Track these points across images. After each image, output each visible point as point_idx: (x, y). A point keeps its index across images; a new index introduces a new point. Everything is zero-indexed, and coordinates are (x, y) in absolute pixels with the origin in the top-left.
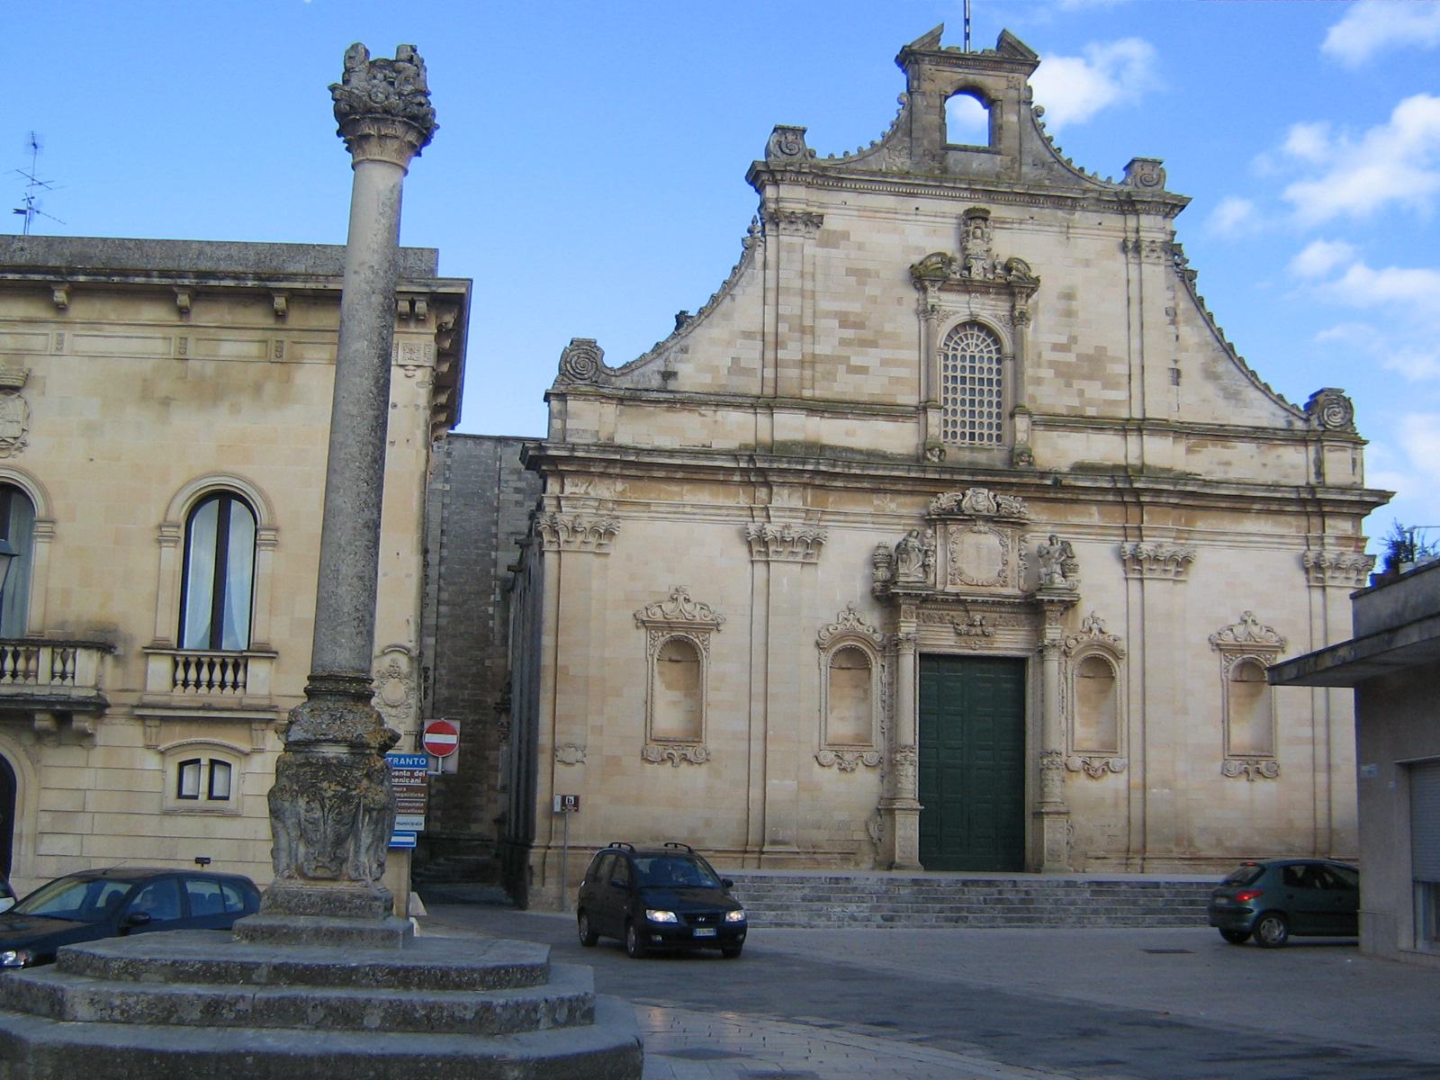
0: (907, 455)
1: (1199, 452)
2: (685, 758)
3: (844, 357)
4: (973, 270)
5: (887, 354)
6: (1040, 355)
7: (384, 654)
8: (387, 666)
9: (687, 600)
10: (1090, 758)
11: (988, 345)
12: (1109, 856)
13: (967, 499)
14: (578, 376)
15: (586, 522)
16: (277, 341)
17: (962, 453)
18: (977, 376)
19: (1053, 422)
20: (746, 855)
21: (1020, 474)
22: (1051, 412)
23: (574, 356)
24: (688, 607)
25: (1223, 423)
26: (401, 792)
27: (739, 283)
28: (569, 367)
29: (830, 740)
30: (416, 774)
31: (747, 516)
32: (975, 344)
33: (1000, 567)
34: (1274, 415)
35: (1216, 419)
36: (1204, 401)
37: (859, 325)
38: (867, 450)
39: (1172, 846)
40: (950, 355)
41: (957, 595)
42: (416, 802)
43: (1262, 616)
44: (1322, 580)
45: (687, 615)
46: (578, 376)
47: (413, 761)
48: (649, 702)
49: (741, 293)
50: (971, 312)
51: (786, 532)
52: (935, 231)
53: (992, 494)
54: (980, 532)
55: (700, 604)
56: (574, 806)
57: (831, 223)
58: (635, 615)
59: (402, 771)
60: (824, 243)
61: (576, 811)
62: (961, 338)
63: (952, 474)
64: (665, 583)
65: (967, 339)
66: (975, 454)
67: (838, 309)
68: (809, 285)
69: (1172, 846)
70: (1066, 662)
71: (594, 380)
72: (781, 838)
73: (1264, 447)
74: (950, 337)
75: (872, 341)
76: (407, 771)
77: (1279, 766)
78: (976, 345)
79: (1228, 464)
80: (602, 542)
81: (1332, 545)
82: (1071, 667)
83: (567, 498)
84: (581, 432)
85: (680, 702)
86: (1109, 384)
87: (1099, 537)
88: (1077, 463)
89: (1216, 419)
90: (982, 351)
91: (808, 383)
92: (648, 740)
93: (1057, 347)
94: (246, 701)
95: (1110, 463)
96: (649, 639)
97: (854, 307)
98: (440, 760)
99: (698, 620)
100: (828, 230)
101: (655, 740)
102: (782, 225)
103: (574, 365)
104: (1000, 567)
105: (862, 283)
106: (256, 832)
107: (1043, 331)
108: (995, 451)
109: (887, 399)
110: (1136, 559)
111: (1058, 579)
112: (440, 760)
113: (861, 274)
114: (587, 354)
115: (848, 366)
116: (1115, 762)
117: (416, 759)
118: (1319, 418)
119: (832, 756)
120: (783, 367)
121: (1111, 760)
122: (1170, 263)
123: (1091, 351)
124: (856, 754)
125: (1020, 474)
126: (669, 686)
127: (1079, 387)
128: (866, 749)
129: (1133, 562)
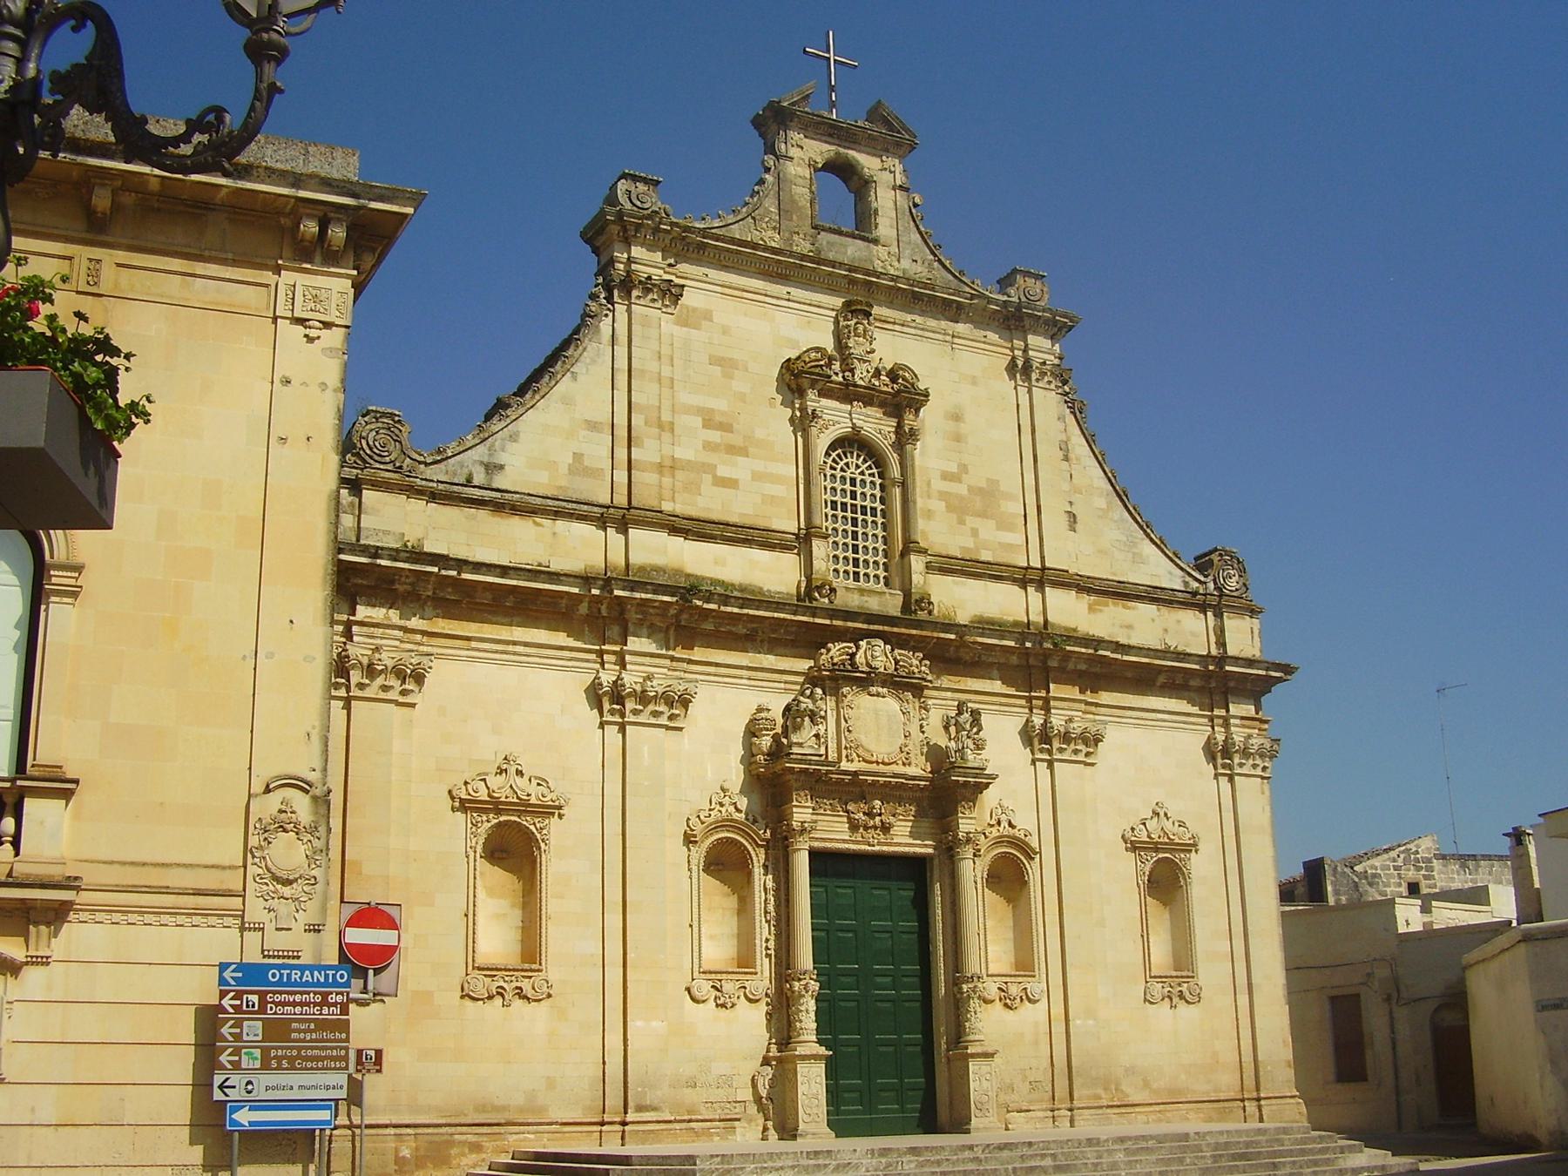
0: (788, 594)
1: (1101, 611)
2: (520, 993)
3: (709, 465)
4: (857, 372)
5: (759, 465)
6: (929, 484)
7: (268, 790)
8: (275, 812)
9: (520, 773)
10: (1006, 983)
11: (870, 467)
12: (1032, 1108)
13: (861, 652)
14: (376, 458)
15: (387, 659)
16: (90, 260)
17: (850, 595)
18: (858, 502)
19: (948, 566)
20: (604, 1128)
21: (919, 624)
22: (944, 553)
23: (372, 430)
24: (521, 783)
25: (1121, 579)
26: (304, 1031)
27: (582, 358)
28: (365, 446)
29: (705, 967)
30: (332, 998)
31: (595, 662)
32: (855, 464)
33: (902, 740)
34: (1170, 573)
35: (1115, 575)
36: (1100, 551)
37: (725, 427)
38: (740, 585)
39: (1100, 1091)
40: (828, 474)
41: (855, 774)
42: (332, 1048)
43: (1175, 808)
44: (1230, 767)
45: (519, 792)
46: (376, 458)
47: (327, 976)
48: (470, 916)
49: (584, 371)
50: (853, 424)
51: (649, 683)
52: (809, 322)
53: (888, 647)
54: (878, 695)
55: (536, 778)
56: (375, 1064)
57: (690, 298)
58: (450, 792)
59: (308, 993)
60: (684, 322)
61: (379, 1071)
62: (838, 455)
63: (831, 619)
64: (489, 751)
65: (846, 458)
66: (866, 598)
67: (701, 405)
68: (666, 371)
69: (1100, 1091)
70: (974, 863)
71: (398, 465)
72: (648, 1103)
73: (1164, 609)
74: (827, 454)
75: (741, 448)
76: (315, 993)
77: (1201, 989)
78: (857, 465)
79: (1130, 627)
80: (406, 686)
81: (1237, 726)
82: (980, 868)
83: (361, 624)
84: (381, 534)
85: (504, 915)
86: (1003, 525)
87: (1002, 708)
88: (975, 616)
89: (1115, 575)
90: (862, 473)
91: (667, 493)
92: (470, 968)
93: (946, 476)
94: (21, 869)
95: (1011, 619)
96: (469, 825)
97: (720, 404)
98: (371, 972)
99: (533, 800)
100: (687, 307)
101: (479, 969)
102: (635, 293)
103: (371, 443)
104: (902, 740)
105: (729, 377)
106: (33, 1110)
107: (929, 457)
108: (887, 595)
109: (761, 523)
110: (1046, 736)
111: (970, 755)
112: (371, 972)
113: (726, 364)
114: (389, 429)
115: (715, 476)
116: (1036, 987)
117: (330, 973)
118: (1214, 580)
119: (707, 986)
120: (638, 470)
121: (1028, 986)
122: (1060, 391)
123: (983, 484)
124: (738, 985)
125: (919, 624)
126: (491, 892)
127: (974, 526)
128: (748, 977)
129: (1038, 739)
